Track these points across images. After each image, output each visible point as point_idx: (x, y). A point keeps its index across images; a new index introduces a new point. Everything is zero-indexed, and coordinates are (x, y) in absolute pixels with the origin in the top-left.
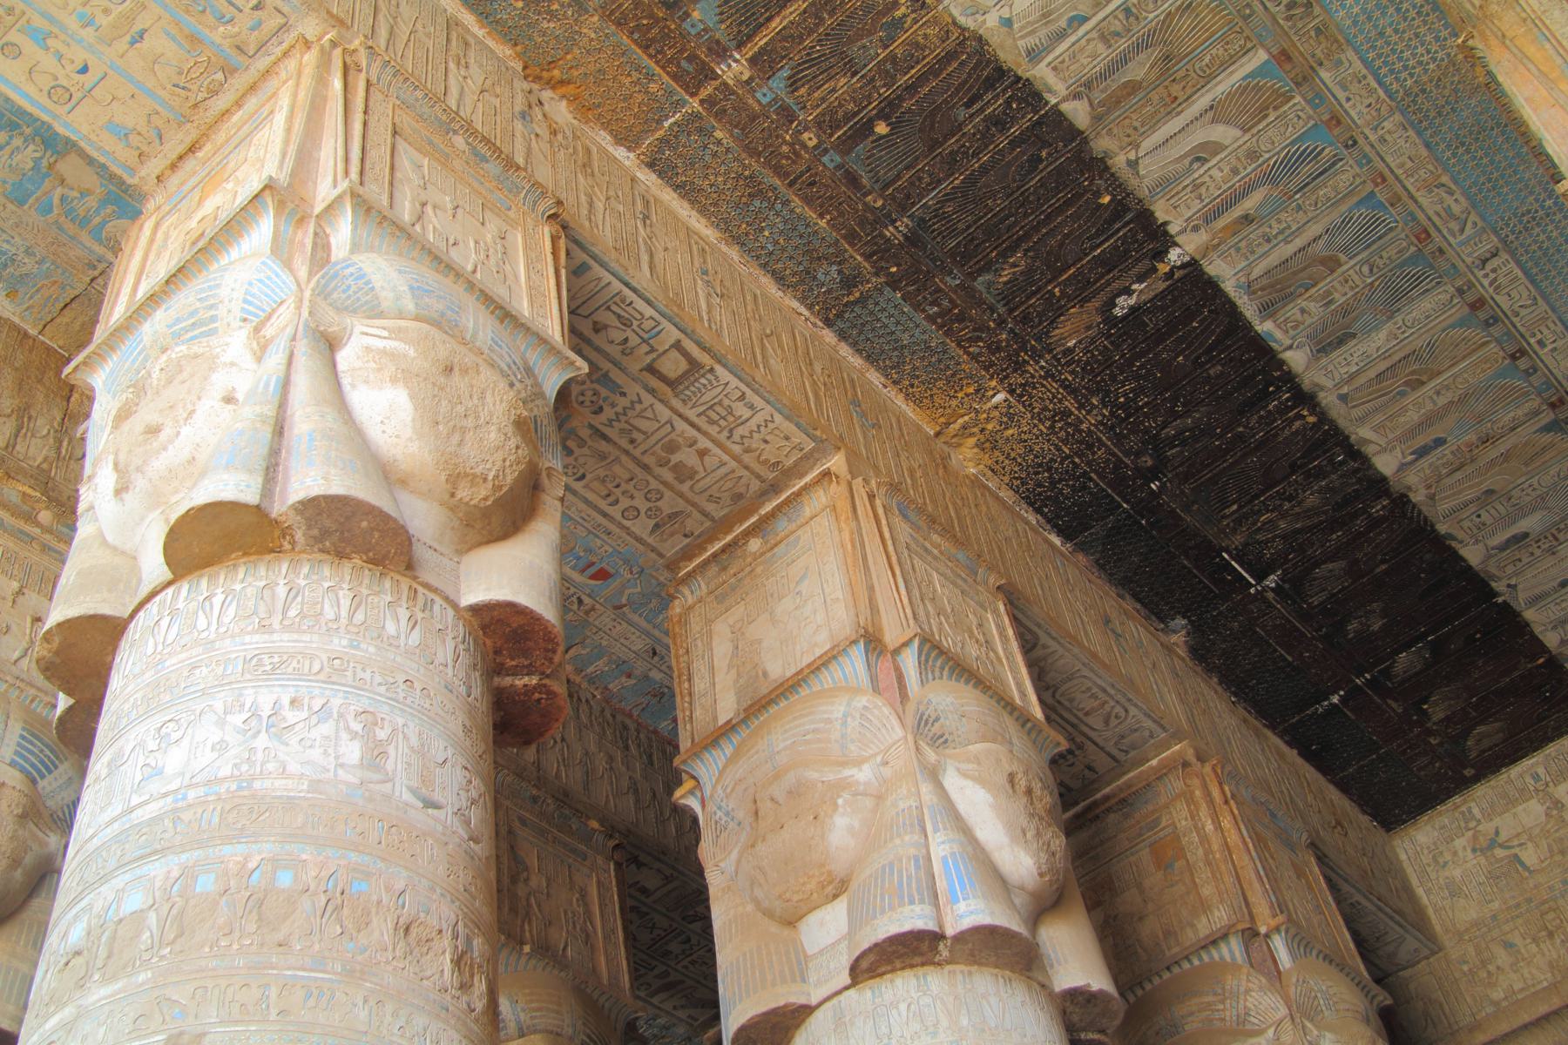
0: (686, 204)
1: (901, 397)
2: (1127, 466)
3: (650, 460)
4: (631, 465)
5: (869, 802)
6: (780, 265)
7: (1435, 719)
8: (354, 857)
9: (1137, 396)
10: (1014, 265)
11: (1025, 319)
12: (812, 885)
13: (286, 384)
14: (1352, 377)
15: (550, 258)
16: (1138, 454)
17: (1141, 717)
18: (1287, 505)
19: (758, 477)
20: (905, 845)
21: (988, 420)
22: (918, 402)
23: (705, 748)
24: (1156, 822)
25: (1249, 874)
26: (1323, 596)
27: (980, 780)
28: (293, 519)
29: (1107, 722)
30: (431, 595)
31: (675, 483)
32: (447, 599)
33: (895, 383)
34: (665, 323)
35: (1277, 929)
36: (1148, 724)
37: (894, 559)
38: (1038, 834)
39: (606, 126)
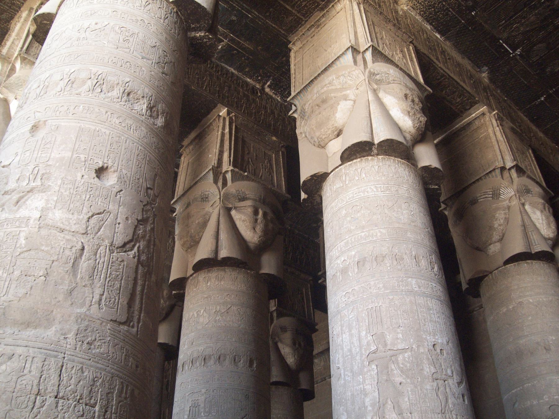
12: (329, 132)
38: (414, 114)
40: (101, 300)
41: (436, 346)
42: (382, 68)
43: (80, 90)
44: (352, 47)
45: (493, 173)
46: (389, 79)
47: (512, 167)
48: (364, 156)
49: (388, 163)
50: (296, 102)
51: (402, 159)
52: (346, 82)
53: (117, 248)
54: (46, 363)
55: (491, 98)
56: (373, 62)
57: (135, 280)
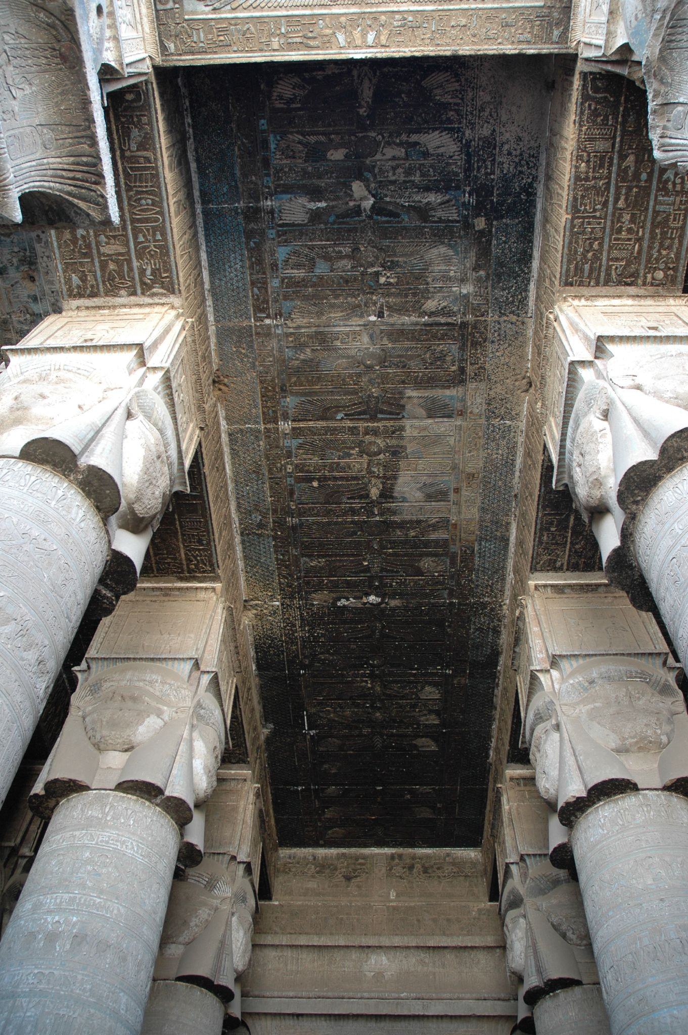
0: (230, 457)
1: (245, 578)
2: (299, 658)
6: (243, 502)
7: (326, 816)
9: (322, 636)
10: (319, 562)
11: (308, 583)
16: (306, 657)
18: (338, 709)
21: (266, 609)
22: (248, 585)
26: (325, 749)
33: (246, 572)
39: (227, 410)
42: (210, 701)
44: (197, 660)
45: (221, 857)
46: (210, 720)
47: (243, 863)
48: (142, 798)
49: (162, 821)
50: (93, 665)
51: (176, 823)
52: (168, 695)
55: (258, 761)
56: (206, 691)
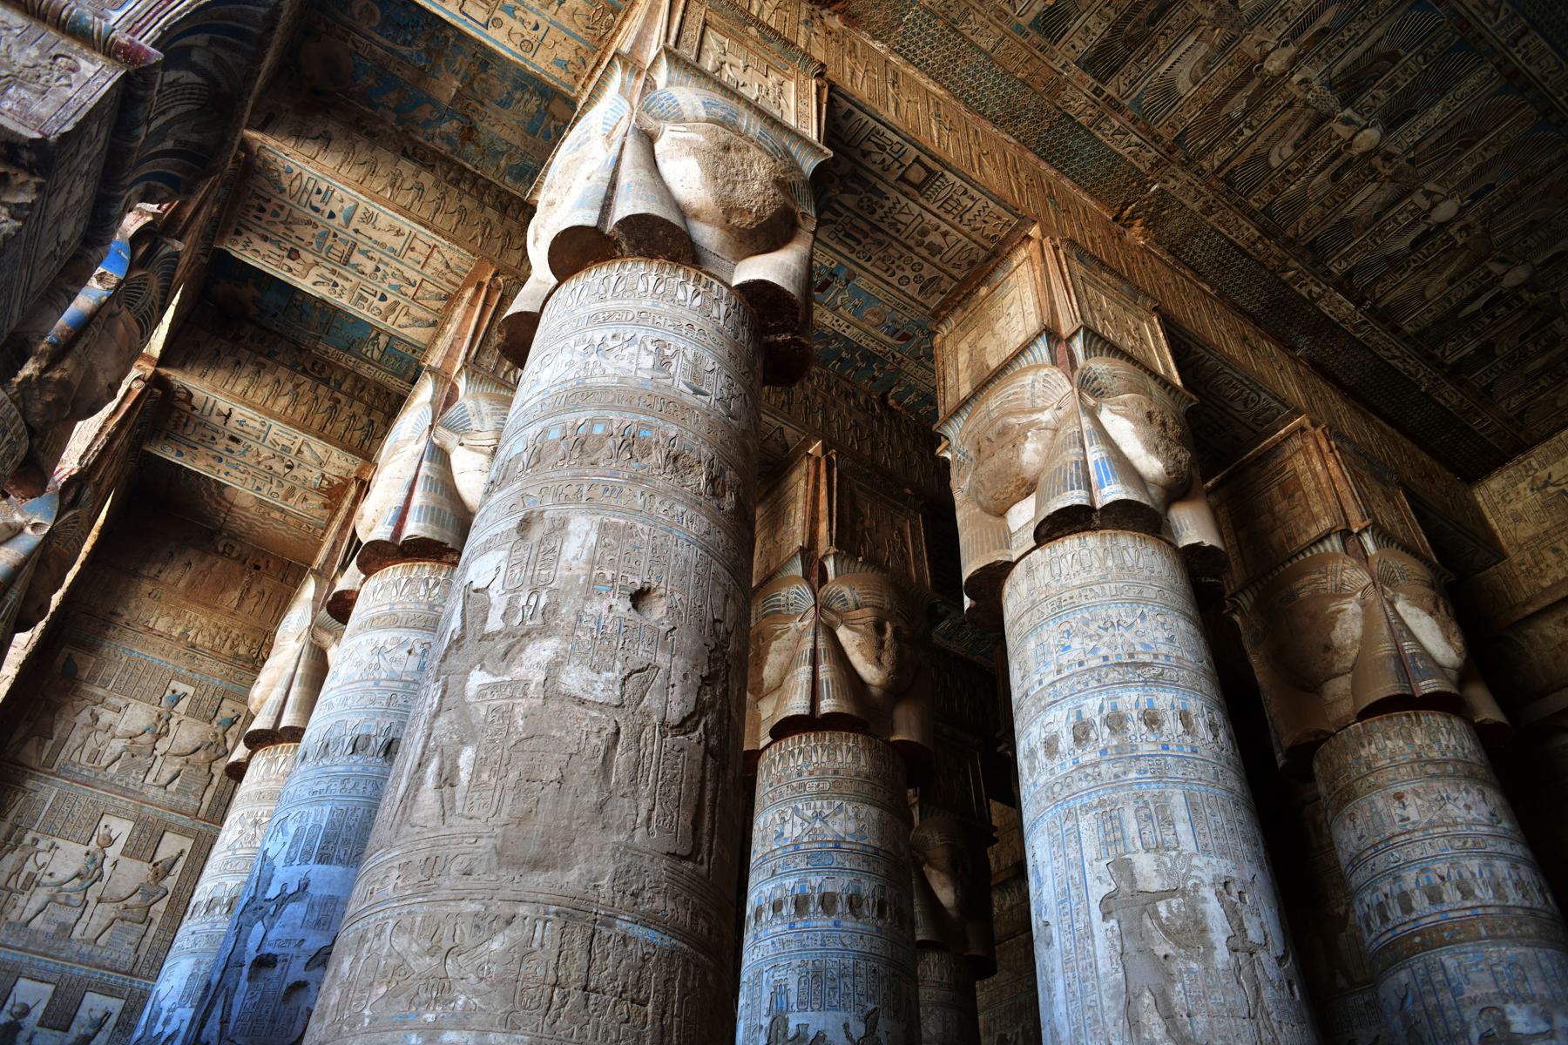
3: (910, 242)
4: (900, 248)
5: (1049, 434)
8: (643, 418)
13: (619, 160)
14: (1416, 144)
15: (814, 96)
17: (1270, 399)
19: (983, 247)
20: (1073, 454)
21: (1149, 206)
23: (951, 417)
24: (1284, 468)
25: (1346, 495)
27: (1126, 416)
28: (619, 234)
29: (1246, 405)
30: (711, 279)
31: (930, 257)
32: (722, 281)
34: (908, 145)
35: (1366, 529)
36: (1275, 404)
37: (1070, 284)
38: (1167, 449)
40: (649, 819)
41: (1231, 885)
42: (1101, 366)
43: (596, 456)
53: (672, 728)
54: (567, 930)
57: (703, 781)
